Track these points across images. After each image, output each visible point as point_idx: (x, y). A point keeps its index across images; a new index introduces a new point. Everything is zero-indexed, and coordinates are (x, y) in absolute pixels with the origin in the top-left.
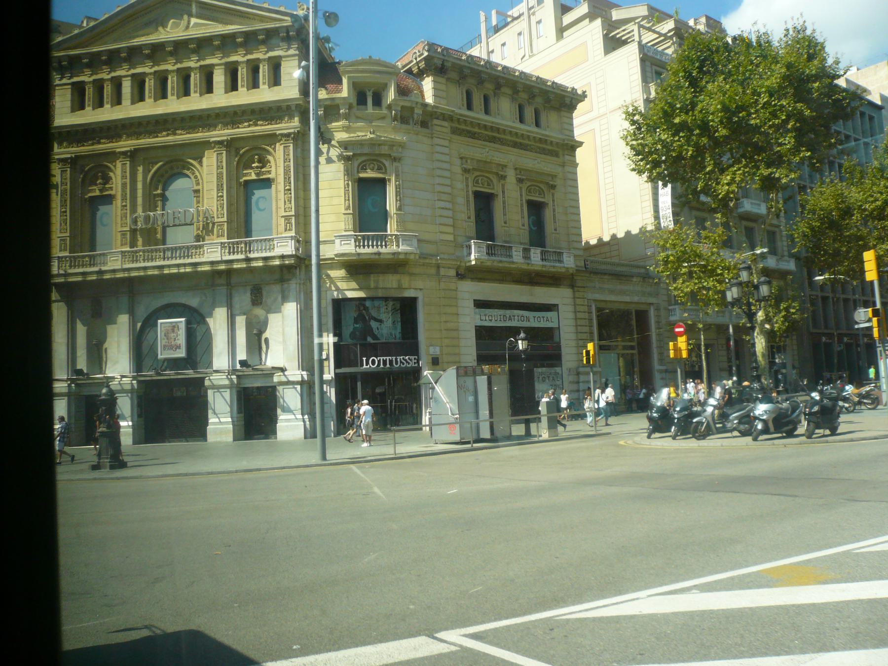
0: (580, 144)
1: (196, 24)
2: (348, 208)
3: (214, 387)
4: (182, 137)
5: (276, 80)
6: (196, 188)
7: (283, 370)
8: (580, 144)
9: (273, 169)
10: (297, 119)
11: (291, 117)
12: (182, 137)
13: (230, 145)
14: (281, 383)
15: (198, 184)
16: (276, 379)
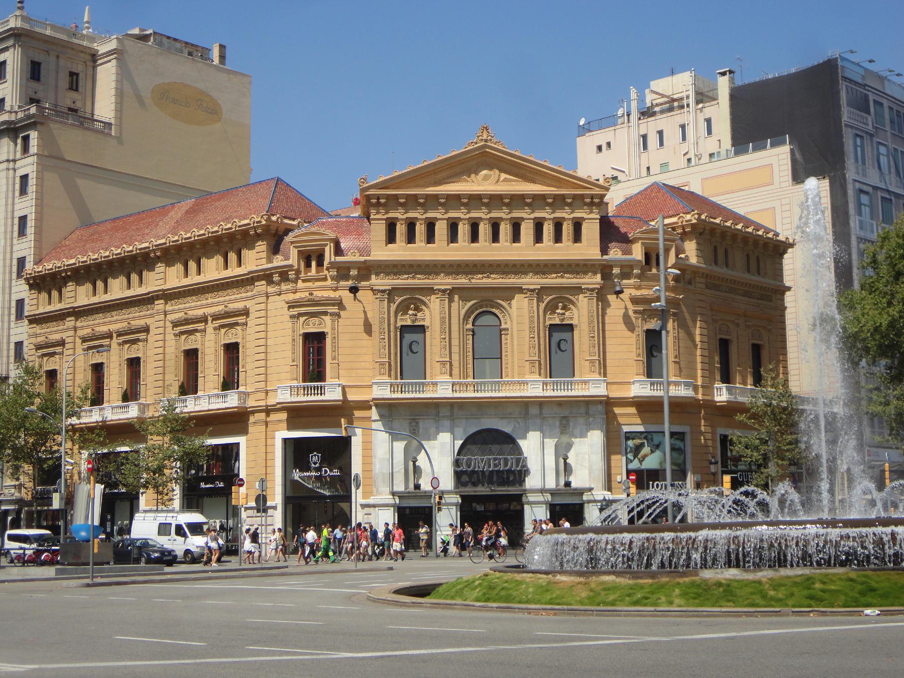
0: (789, 289)
1: (505, 180)
2: (639, 355)
3: (529, 503)
4: (496, 280)
5: (577, 237)
6: (503, 326)
7: (590, 489)
8: (789, 289)
9: (576, 316)
10: (599, 276)
11: (595, 273)
12: (496, 280)
13: (541, 292)
14: (589, 502)
15: (506, 323)
16: (585, 498)
